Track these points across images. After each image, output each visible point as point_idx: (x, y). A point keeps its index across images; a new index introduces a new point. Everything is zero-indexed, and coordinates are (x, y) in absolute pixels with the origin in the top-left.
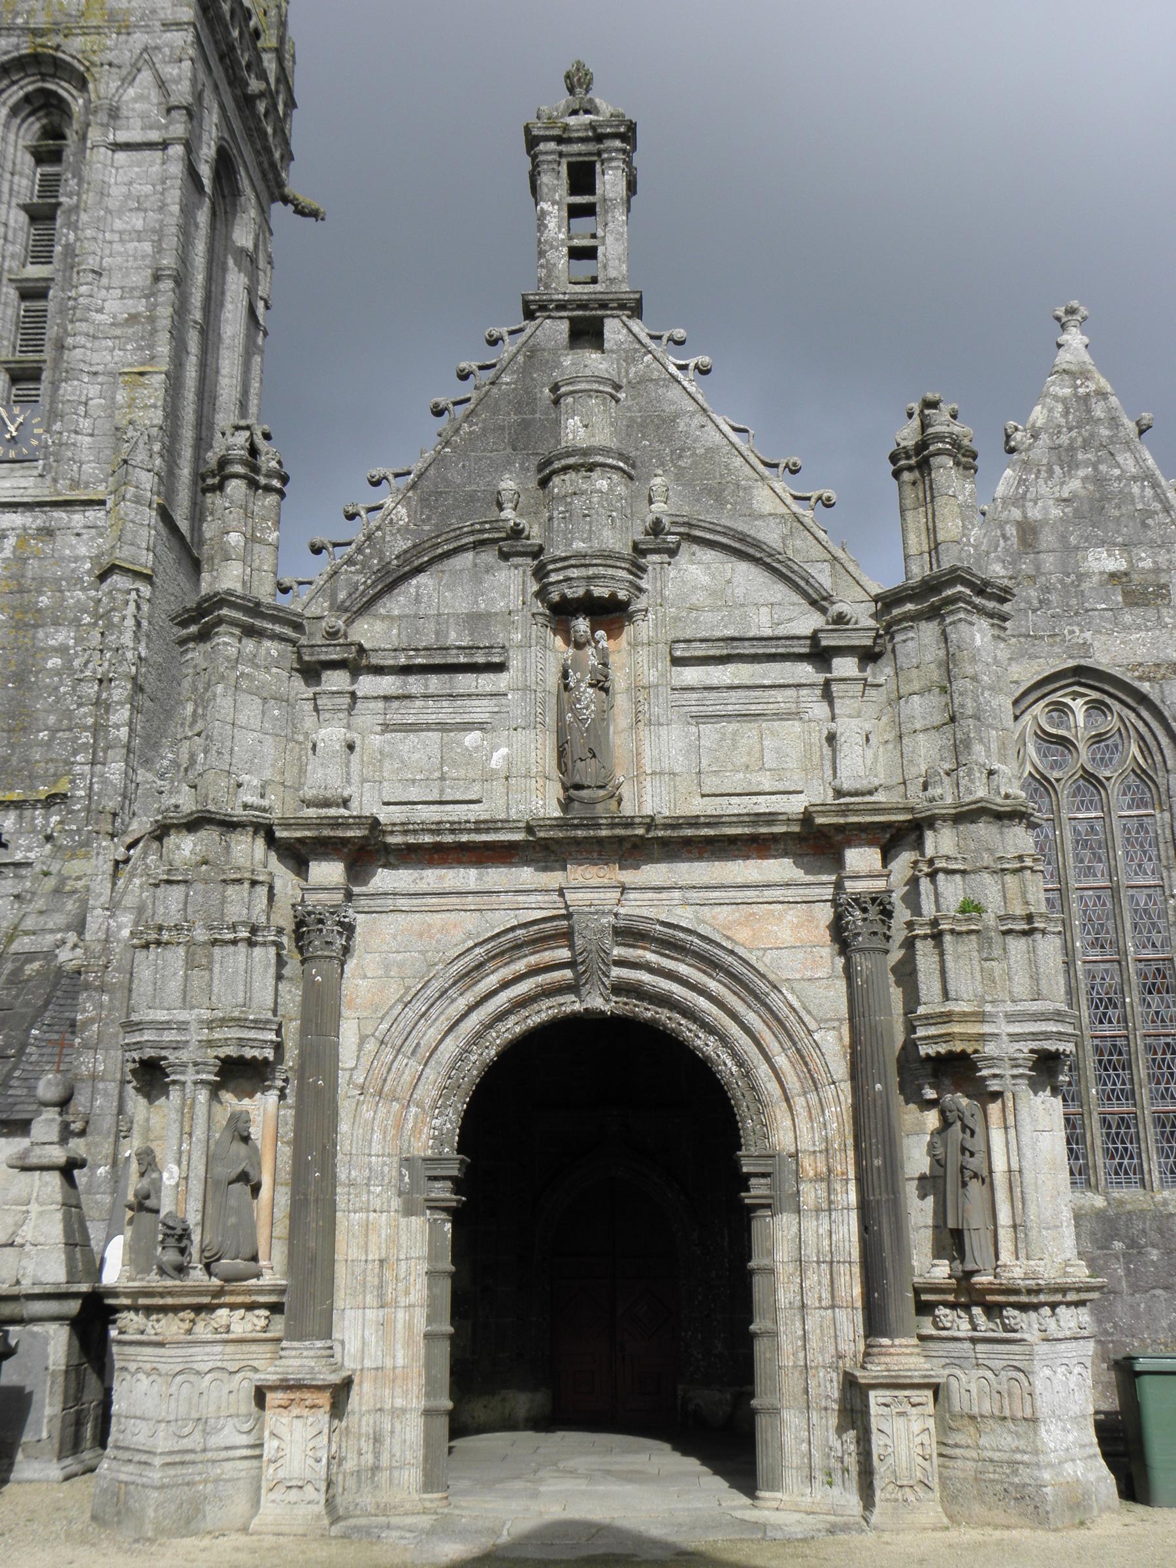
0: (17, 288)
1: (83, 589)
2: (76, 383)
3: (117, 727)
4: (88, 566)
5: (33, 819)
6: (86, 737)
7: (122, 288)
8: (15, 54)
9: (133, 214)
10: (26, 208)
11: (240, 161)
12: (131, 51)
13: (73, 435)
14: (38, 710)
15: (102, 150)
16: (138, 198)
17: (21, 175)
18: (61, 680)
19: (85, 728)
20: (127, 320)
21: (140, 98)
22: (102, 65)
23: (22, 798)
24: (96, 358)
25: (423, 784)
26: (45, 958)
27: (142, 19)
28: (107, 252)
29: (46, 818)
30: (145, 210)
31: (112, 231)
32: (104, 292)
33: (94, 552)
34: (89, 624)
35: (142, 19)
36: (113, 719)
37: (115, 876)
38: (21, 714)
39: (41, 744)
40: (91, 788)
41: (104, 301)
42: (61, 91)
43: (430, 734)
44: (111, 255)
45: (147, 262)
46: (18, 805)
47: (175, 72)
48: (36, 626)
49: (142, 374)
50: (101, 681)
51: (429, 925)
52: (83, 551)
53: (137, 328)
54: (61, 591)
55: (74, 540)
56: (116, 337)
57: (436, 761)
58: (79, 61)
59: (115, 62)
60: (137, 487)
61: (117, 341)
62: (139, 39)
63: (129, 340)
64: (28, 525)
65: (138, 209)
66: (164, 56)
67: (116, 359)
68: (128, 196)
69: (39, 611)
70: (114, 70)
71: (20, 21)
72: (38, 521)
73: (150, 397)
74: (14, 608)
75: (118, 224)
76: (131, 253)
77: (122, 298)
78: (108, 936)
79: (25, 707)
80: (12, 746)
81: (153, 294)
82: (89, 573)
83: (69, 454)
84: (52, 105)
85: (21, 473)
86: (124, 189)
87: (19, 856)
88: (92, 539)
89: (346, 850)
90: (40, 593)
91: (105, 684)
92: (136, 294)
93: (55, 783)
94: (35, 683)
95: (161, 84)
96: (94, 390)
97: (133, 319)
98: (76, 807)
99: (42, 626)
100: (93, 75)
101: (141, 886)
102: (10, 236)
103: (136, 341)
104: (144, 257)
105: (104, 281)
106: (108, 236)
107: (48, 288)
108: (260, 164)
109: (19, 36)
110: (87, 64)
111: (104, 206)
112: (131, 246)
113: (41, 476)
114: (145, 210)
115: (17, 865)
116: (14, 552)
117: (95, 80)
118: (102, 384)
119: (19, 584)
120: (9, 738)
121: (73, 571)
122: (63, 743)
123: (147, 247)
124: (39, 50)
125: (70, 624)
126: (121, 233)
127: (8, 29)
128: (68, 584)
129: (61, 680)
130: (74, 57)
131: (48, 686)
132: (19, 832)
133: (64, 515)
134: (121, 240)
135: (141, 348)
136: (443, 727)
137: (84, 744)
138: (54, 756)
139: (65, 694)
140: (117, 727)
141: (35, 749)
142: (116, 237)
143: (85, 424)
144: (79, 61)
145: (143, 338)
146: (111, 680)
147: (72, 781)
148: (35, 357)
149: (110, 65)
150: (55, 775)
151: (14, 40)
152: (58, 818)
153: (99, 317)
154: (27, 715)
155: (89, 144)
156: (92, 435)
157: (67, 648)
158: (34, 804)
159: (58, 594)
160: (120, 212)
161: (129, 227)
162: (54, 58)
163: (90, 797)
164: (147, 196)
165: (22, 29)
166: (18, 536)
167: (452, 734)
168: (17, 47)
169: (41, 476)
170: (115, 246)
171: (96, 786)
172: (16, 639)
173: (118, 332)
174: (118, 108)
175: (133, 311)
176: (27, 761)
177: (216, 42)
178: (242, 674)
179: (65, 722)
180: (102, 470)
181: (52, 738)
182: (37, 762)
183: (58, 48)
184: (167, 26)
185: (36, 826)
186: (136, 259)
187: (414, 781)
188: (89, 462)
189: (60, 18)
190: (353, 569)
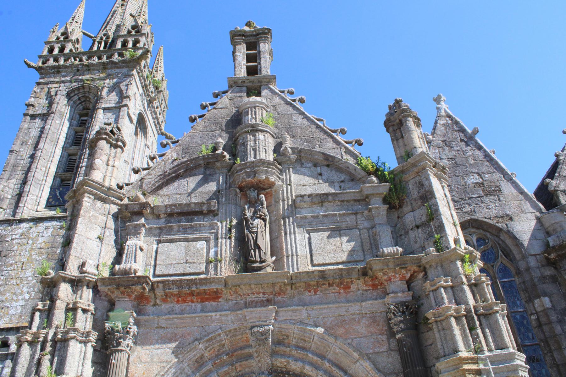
11: (147, 119)
17: (74, 120)
25: (176, 266)
43: (180, 243)
51: (176, 334)
57: (183, 255)
84: (88, 101)
89: (134, 295)
108: (154, 122)
136: (187, 240)
167: (191, 243)
177: (141, 83)
178: (93, 216)
187: (171, 264)
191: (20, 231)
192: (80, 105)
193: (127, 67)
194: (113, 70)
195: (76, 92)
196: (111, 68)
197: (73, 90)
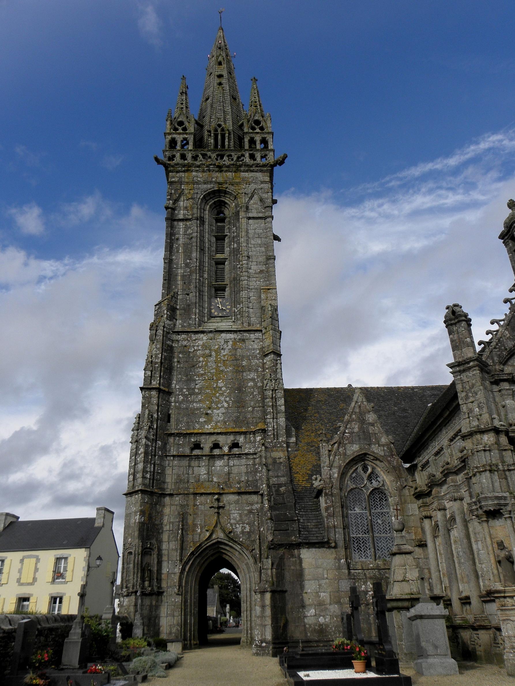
0: (215, 261)
1: (257, 359)
3: (280, 406)
4: (258, 352)
5: (250, 438)
6: (270, 409)
7: (256, 262)
8: (213, 189)
10: (215, 236)
14: (247, 400)
15: (245, 219)
16: (258, 234)
18: (254, 390)
19: (269, 406)
21: (254, 204)
23: (246, 430)
26: (285, 486)
27: (253, 180)
29: (254, 437)
30: (261, 238)
31: (251, 244)
32: (250, 263)
33: (260, 347)
34: (261, 371)
35: (253, 180)
36: (278, 403)
37: (329, 456)
38: (241, 402)
39: (249, 412)
40: (274, 427)
42: (226, 201)
44: (251, 252)
45: (264, 254)
46: (245, 433)
47: (266, 196)
48: (243, 372)
49: (269, 289)
50: (272, 390)
52: (256, 346)
54: (250, 360)
55: (252, 343)
61: (257, 279)
62: (253, 186)
63: (261, 278)
64: (236, 338)
65: (258, 237)
67: (257, 284)
68: (255, 233)
69: (243, 366)
71: (214, 180)
74: (234, 365)
75: (253, 242)
76: (258, 251)
77: (257, 265)
78: (330, 477)
79: (242, 399)
80: (240, 413)
81: (267, 264)
82: (259, 353)
85: (225, 321)
86: (253, 231)
87: (246, 451)
90: (242, 361)
91: (274, 391)
92: (261, 264)
93: (256, 425)
94: (245, 391)
95: (261, 200)
97: (261, 272)
98: (269, 434)
99: (245, 372)
101: (339, 459)
102: (212, 245)
103: (264, 279)
104: (263, 252)
105: (251, 260)
107: (225, 261)
109: (214, 184)
112: (258, 249)
113: (234, 322)
114: (261, 238)
115: (246, 454)
116: (232, 347)
119: (235, 357)
120: (238, 410)
121: (253, 353)
122: (257, 411)
123: (263, 249)
124: (221, 188)
125: (254, 371)
127: (211, 182)
128: (252, 358)
129: (254, 390)
131: (249, 392)
132: (246, 443)
133: (248, 335)
134: (254, 247)
135: (266, 281)
137: (269, 412)
138: (255, 416)
139: (256, 395)
140: (280, 406)
141: (248, 414)
142: (253, 246)
145: (266, 278)
146: (276, 390)
147: (267, 425)
148: (223, 283)
149: (245, 193)
150: (256, 422)
151: (212, 185)
152: (261, 438)
153: (250, 271)
154: (243, 402)
155: (240, 217)
156: (252, 309)
157: (255, 379)
158: (250, 433)
159: (249, 361)
160: (253, 238)
161: (256, 243)
162: (225, 191)
163: (274, 430)
164: (261, 233)
165: (215, 182)
166: (232, 341)
168: (213, 188)
169: (234, 322)
170: (252, 248)
171: (275, 426)
172: (236, 376)
173: (257, 276)
174: (248, 207)
175: (261, 269)
176: (246, 418)
179: (257, 404)
180: (257, 320)
181: (253, 410)
182: (249, 418)
183: (227, 188)
184: (262, 182)
185: (251, 440)
186: (260, 253)
188: (253, 317)
189: (226, 179)
190: (496, 350)
191: (201, 343)
193: (260, 172)
194: (247, 174)
195: (212, 196)
196: (244, 171)
197: (209, 194)
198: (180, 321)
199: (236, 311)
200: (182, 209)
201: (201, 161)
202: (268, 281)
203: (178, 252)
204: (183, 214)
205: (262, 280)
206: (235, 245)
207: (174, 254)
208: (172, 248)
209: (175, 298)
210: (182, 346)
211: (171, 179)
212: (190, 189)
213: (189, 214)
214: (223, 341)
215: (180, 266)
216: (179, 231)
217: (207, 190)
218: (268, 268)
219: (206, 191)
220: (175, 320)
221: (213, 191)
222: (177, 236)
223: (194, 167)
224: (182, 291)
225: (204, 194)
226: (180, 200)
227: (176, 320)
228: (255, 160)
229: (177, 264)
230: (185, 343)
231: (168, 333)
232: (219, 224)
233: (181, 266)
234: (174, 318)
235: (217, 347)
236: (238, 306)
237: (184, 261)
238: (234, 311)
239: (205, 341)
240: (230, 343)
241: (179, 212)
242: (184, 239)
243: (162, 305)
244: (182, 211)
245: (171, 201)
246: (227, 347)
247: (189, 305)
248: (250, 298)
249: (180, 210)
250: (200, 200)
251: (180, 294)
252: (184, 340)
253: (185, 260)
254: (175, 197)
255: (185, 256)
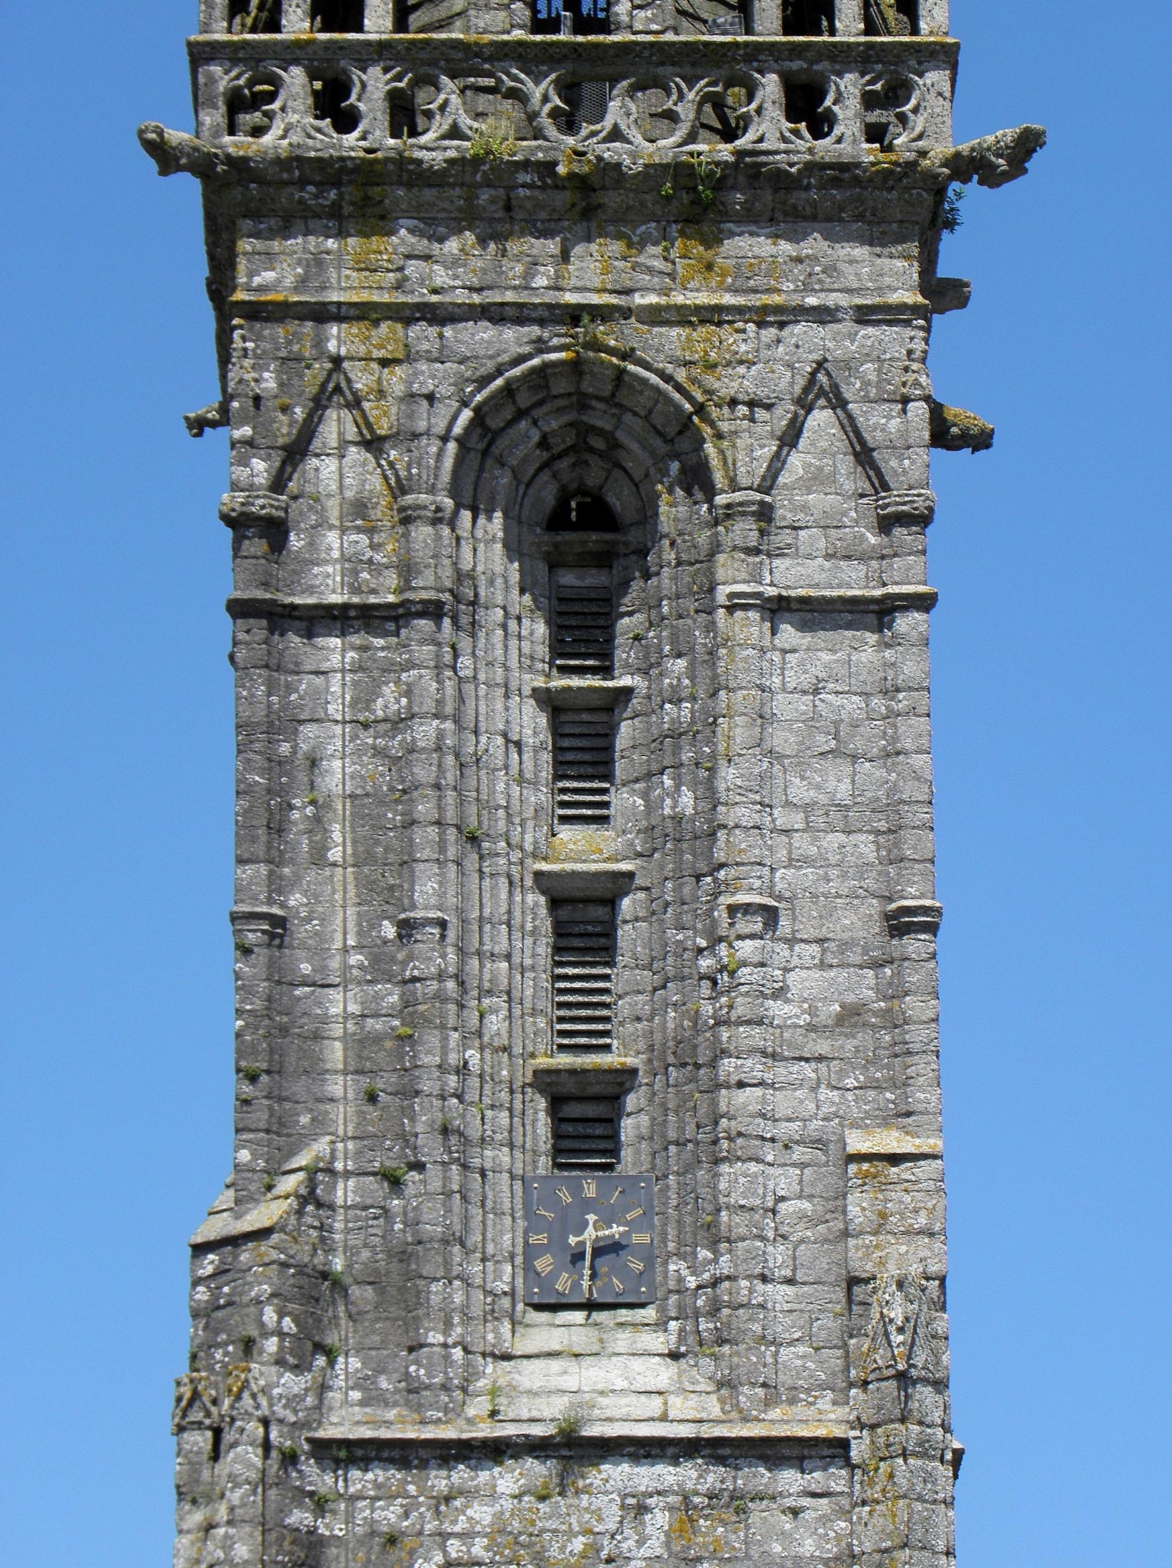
2: (753, 1167)
7: (820, 941)
8: (535, 362)
9: (828, 763)
12: (790, 366)
13: (760, 1287)
16: (837, 724)
20: (840, 1020)
21: (816, 480)
22: (733, 403)
24: (782, 1102)
28: (782, 854)
30: (854, 758)
31: (788, 804)
33: (832, 1549)
41: (786, 970)
44: (791, 863)
47: (894, 424)
49: (895, 1159)
53: (863, 1038)
56: (820, 1059)
58: (679, 388)
59: (762, 393)
60: (920, 1423)
61: (823, 1067)
64: (690, 1485)
66: (866, 384)
67: (825, 1109)
68: (812, 720)
70: (760, 414)
72: (711, 1478)
73: (916, 1211)
75: (799, 791)
76: (833, 859)
77: (823, 966)
83: (756, 1327)
84: (591, 450)
88: (824, 1520)
96: (784, 1181)
97: (851, 1016)
100: (712, 424)
106: (782, 817)
110: (700, 397)
111: (766, 746)
114: (854, 758)
116: (667, 1544)
117: (719, 436)
118: (803, 1166)
123: (865, 847)
126: (808, 808)
130: (668, 379)
143: (778, 1255)
144: (679, 388)
153: (777, 1009)
156: (790, 1281)
160: (801, 765)
161: (823, 799)
164: (855, 725)
166: (671, 1508)
175: (850, 998)
188: (792, 1343)
191: (481, 1514)
192: (545, 476)
198: (355, 1363)
199: (692, 1282)
200: (334, 516)
201: (455, 132)
202: (894, 1085)
203: (319, 858)
204: (344, 558)
205: (850, 1082)
206: (687, 800)
207: (297, 879)
208: (280, 831)
209: (319, 1205)
210: (373, 1533)
211: (251, 274)
212: (384, 363)
213: (378, 557)
214: (615, 1508)
215: (335, 963)
216: (320, 697)
217: (499, 372)
218: (896, 993)
219: (490, 378)
220: (321, 1361)
221: (533, 371)
222: (309, 730)
223: (409, 185)
224: (359, 1153)
225: (479, 398)
226: (316, 445)
227: (331, 1355)
228: (820, 125)
229: (319, 952)
230: (389, 1515)
231: (290, 1459)
232: (568, 578)
233: (346, 967)
234: (319, 1348)
235: (578, 1544)
236: (704, 1254)
237: (360, 933)
238: (681, 1280)
239: (508, 1504)
240: (659, 1520)
241: (312, 544)
242: (359, 753)
243: (244, 1257)
244: (332, 538)
245: (259, 465)
246: (641, 1543)
247: (403, 1255)
248: (774, 1211)
249: (323, 524)
250: (452, 447)
251: (347, 1174)
252: (384, 1494)
253: (367, 925)
254: (285, 429)
255: (367, 887)
